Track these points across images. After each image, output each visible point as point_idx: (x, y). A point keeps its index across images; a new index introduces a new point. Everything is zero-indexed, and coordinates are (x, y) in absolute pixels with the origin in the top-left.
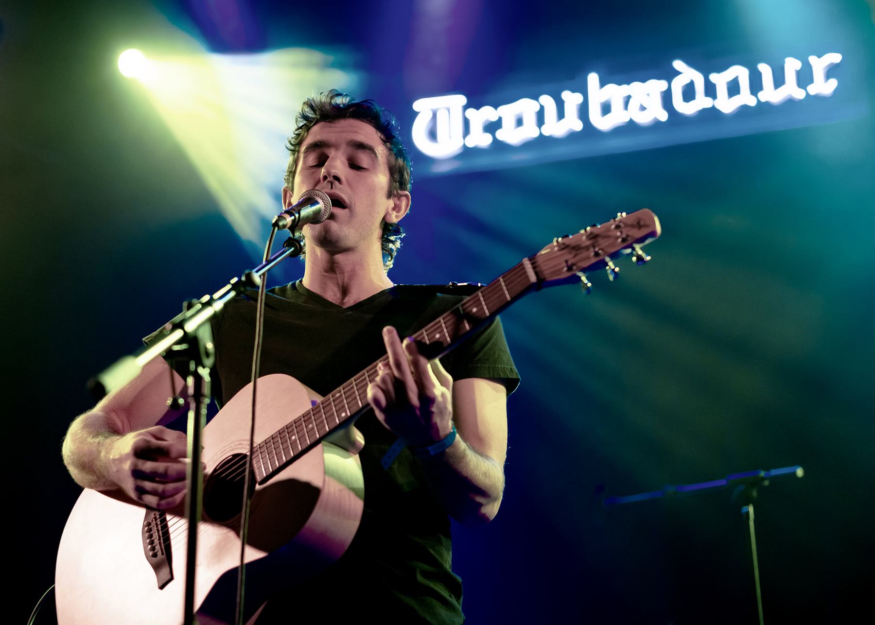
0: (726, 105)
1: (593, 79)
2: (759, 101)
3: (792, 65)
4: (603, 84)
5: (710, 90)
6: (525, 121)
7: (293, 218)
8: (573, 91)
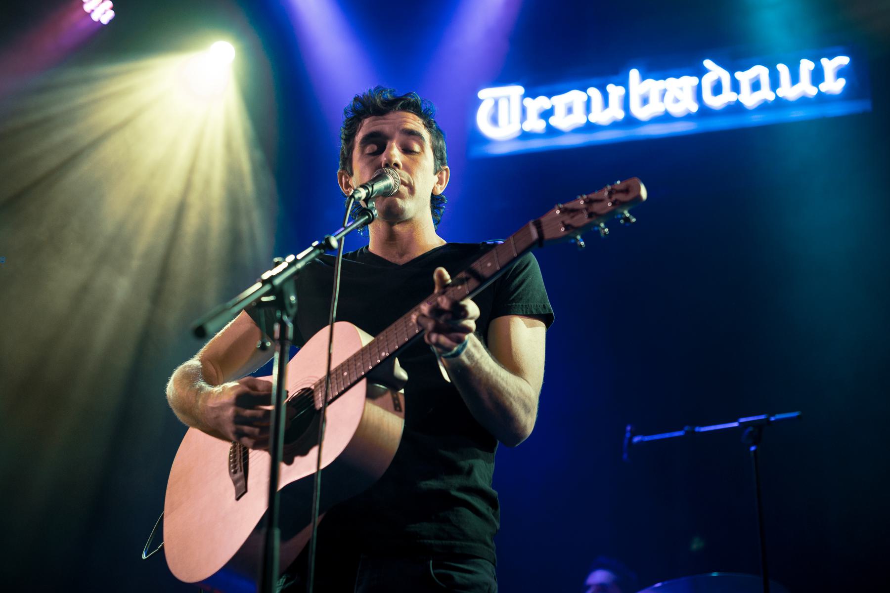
0: (750, 100)
2: (777, 96)
3: (806, 66)
5: (736, 87)
6: (575, 109)
7: (367, 191)
8: (617, 84)
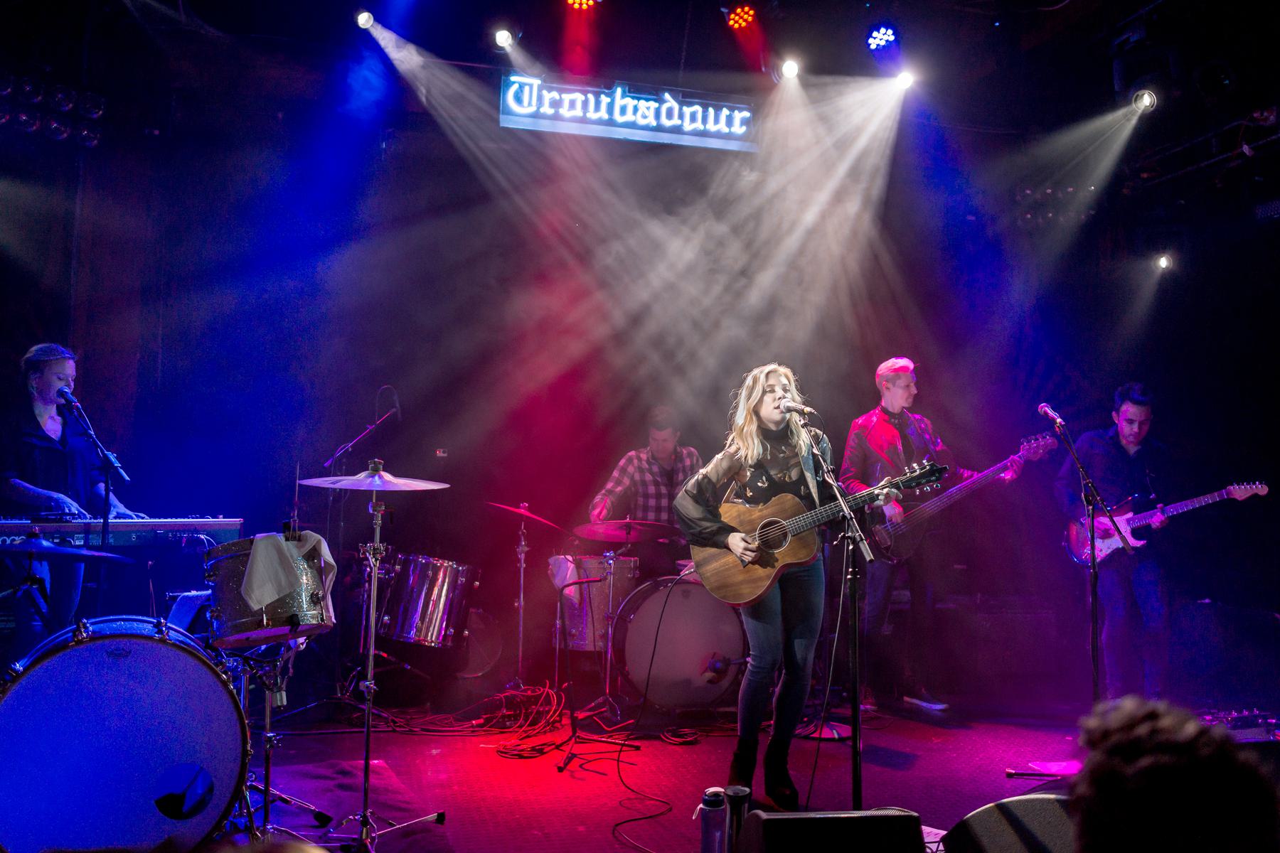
0: (688, 126)
1: (619, 91)
3: (725, 112)
4: (623, 96)
5: (681, 116)
8: (607, 95)
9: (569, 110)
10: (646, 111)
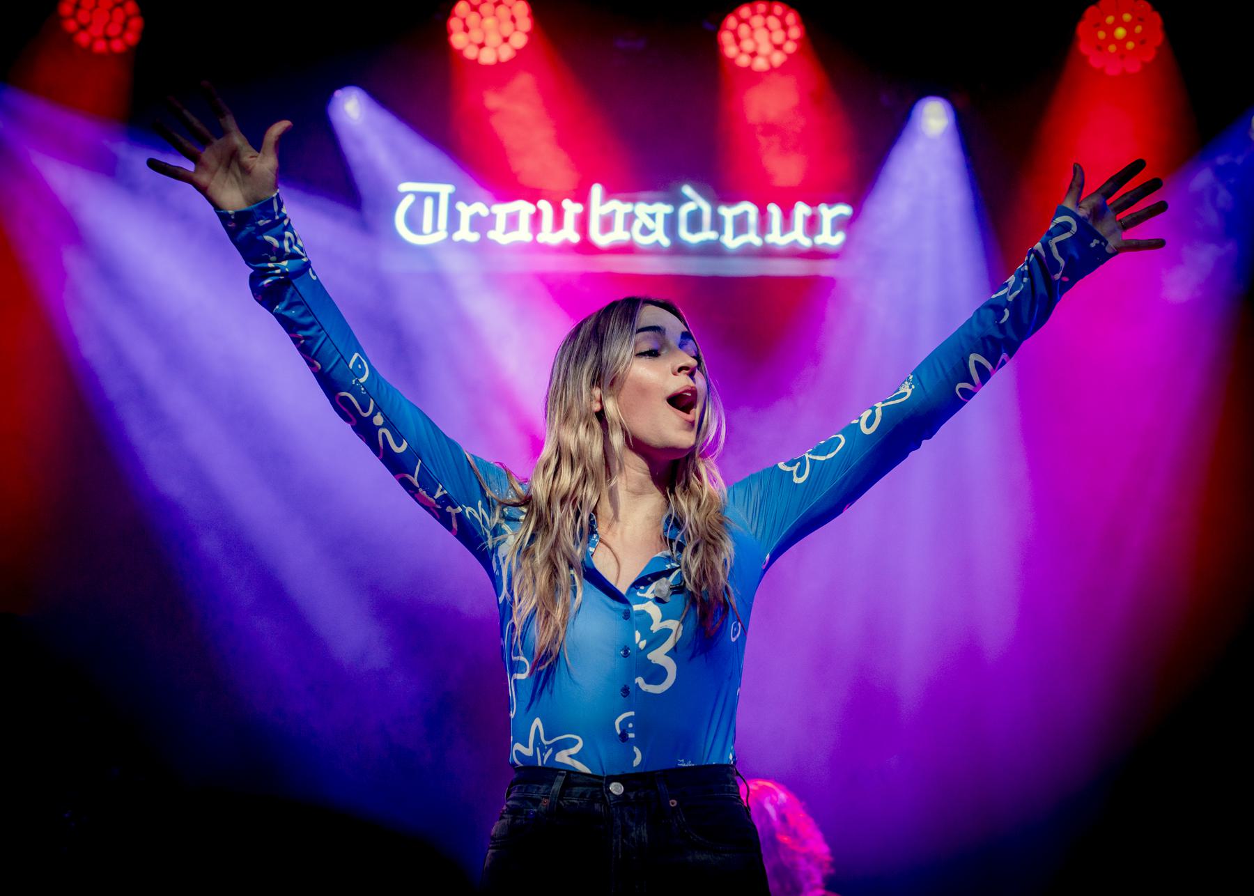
0: (731, 242)
1: (597, 191)
3: (801, 210)
5: (717, 224)
8: (576, 199)
9: (506, 232)
10: (650, 224)
